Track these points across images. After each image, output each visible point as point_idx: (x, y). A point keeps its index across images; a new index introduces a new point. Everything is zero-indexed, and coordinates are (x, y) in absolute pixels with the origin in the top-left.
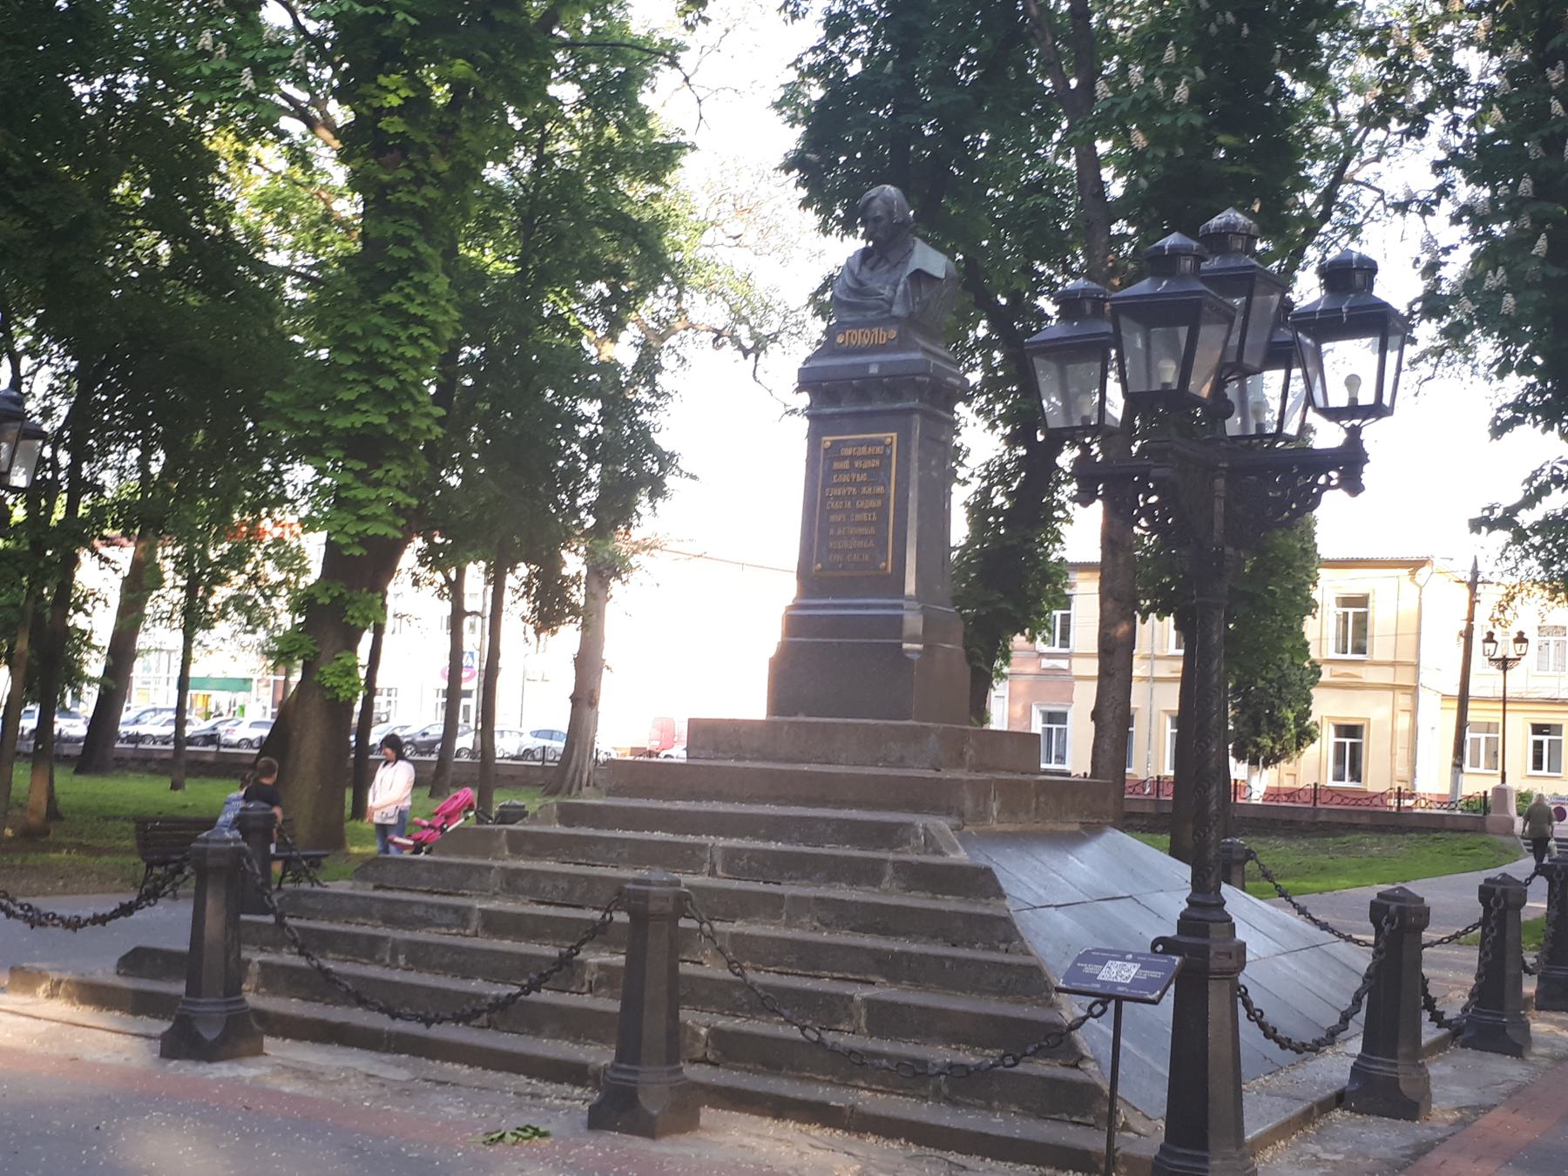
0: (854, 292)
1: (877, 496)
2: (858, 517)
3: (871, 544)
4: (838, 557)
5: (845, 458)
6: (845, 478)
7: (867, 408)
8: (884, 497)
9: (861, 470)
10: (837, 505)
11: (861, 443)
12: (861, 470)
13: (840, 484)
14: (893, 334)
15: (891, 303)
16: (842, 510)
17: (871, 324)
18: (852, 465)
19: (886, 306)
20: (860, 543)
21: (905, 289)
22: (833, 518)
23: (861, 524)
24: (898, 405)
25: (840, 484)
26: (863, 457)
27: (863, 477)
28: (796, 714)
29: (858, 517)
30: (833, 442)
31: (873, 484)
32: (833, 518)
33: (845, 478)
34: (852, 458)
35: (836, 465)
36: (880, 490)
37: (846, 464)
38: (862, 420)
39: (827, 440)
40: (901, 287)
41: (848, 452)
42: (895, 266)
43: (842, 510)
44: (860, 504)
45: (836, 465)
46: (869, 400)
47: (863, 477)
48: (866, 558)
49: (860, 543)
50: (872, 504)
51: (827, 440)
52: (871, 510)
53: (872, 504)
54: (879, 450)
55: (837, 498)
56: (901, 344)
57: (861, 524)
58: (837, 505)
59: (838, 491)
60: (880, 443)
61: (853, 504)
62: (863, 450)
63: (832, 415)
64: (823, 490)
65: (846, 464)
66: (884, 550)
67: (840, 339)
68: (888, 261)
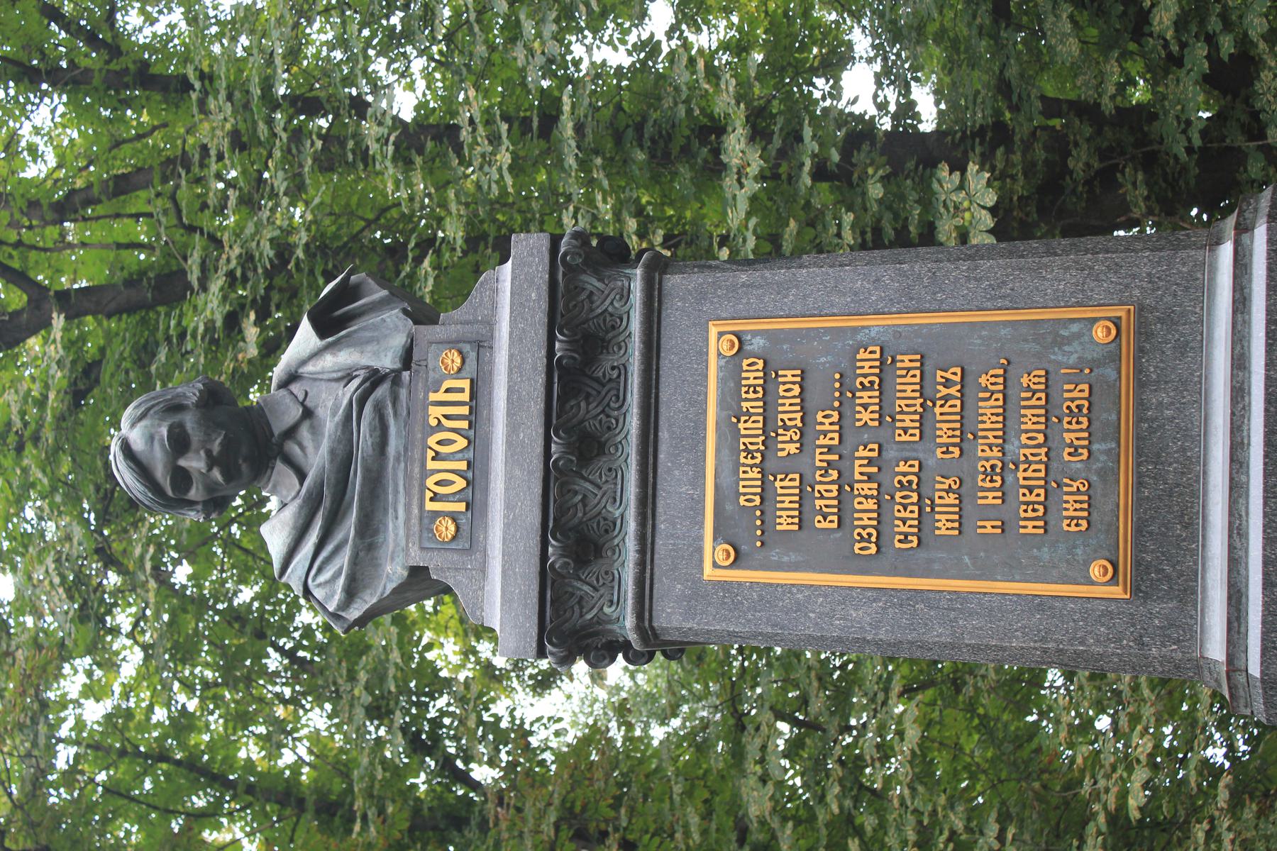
2: (945, 433)
4: (1071, 506)
6: (827, 490)
10: (905, 517)
11: (729, 433)
15: (375, 378)
19: (382, 391)
20: (1030, 419)
22: (944, 525)
27: (826, 421)
29: (945, 433)
35: (785, 522)
36: (867, 364)
37: (786, 487)
39: (714, 561)
42: (308, 413)
45: (785, 522)
47: (826, 421)
50: (907, 387)
53: (907, 387)
54: (752, 377)
58: (905, 517)
60: (732, 368)
62: (751, 428)
65: (786, 487)
66: (1052, 336)
67: (447, 529)
68: (291, 433)
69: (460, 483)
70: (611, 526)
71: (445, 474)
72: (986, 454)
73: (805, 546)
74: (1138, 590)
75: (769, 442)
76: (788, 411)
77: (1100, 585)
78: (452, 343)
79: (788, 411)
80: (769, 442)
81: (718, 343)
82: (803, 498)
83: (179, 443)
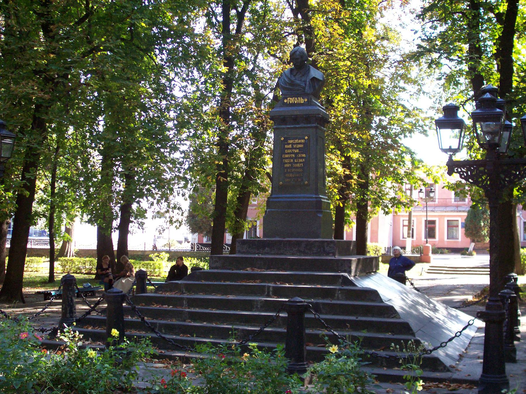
0: (290, 84)
5: (289, 144)
6: (290, 151)
9: (296, 149)
10: (286, 161)
13: (288, 153)
14: (306, 100)
15: (304, 88)
16: (289, 163)
17: (297, 96)
18: (292, 146)
21: (309, 84)
22: (286, 165)
24: (309, 125)
25: (288, 153)
26: (297, 144)
27: (297, 151)
28: (275, 237)
31: (302, 153)
32: (286, 165)
33: (290, 151)
34: (292, 144)
35: (286, 146)
37: (290, 146)
40: (308, 83)
42: (303, 75)
43: (289, 163)
45: (286, 146)
47: (297, 151)
52: (301, 163)
53: (301, 160)
54: (303, 141)
58: (286, 161)
59: (287, 156)
61: (294, 161)
65: (290, 146)
67: (285, 101)
69: (291, 102)
70: (286, 125)
71: (291, 100)
72: (293, 170)
75: (295, 144)
76: (299, 146)
78: (308, 99)
79: (299, 146)
80: (295, 144)
82: (289, 149)
83: (297, 59)
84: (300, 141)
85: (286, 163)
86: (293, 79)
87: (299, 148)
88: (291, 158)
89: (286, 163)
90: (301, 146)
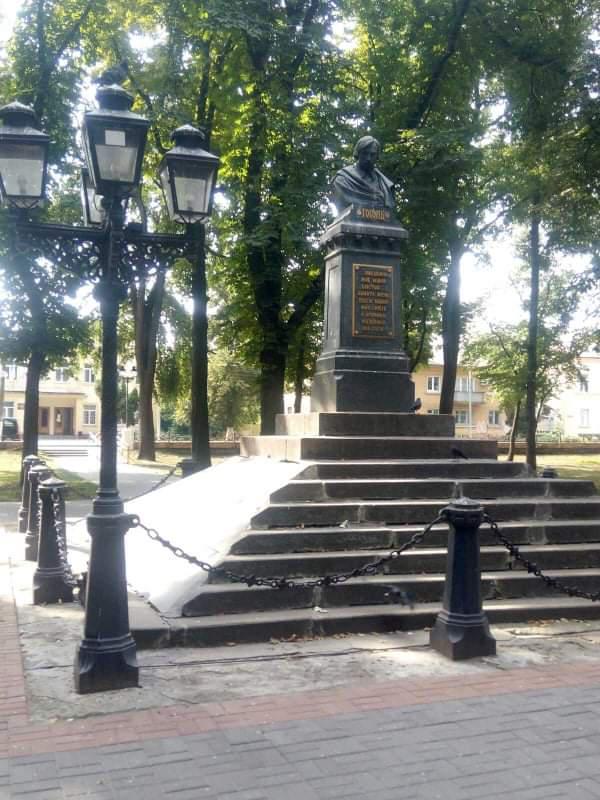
0: (360, 189)
1: (385, 298)
2: (376, 308)
3: (384, 322)
5: (365, 276)
6: (367, 287)
7: (377, 252)
8: (389, 299)
9: (376, 284)
11: (375, 270)
12: (376, 284)
20: (379, 322)
22: (362, 307)
23: (377, 311)
26: (377, 277)
27: (377, 288)
30: (361, 267)
31: (384, 292)
32: (362, 307)
33: (367, 287)
34: (371, 277)
35: (363, 279)
36: (386, 295)
38: (373, 257)
41: (369, 273)
44: (376, 301)
45: (363, 279)
46: (392, 249)
47: (377, 288)
48: (382, 329)
49: (379, 322)
51: (356, 266)
54: (385, 275)
55: (364, 297)
56: (391, 223)
57: (377, 311)
62: (376, 274)
63: (358, 254)
64: (356, 292)
65: (368, 280)
66: (390, 325)
72: (375, 314)
73: (359, 283)
74: (354, 338)
76: (379, 281)
77: (355, 332)
79: (379, 281)
81: (390, 268)
82: (366, 283)
84: (381, 274)
85: (364, 304)
86: (365, 182)
87: (381, 284)
88: (371, 297)
89: (364, 304)
90: (384, 281)
